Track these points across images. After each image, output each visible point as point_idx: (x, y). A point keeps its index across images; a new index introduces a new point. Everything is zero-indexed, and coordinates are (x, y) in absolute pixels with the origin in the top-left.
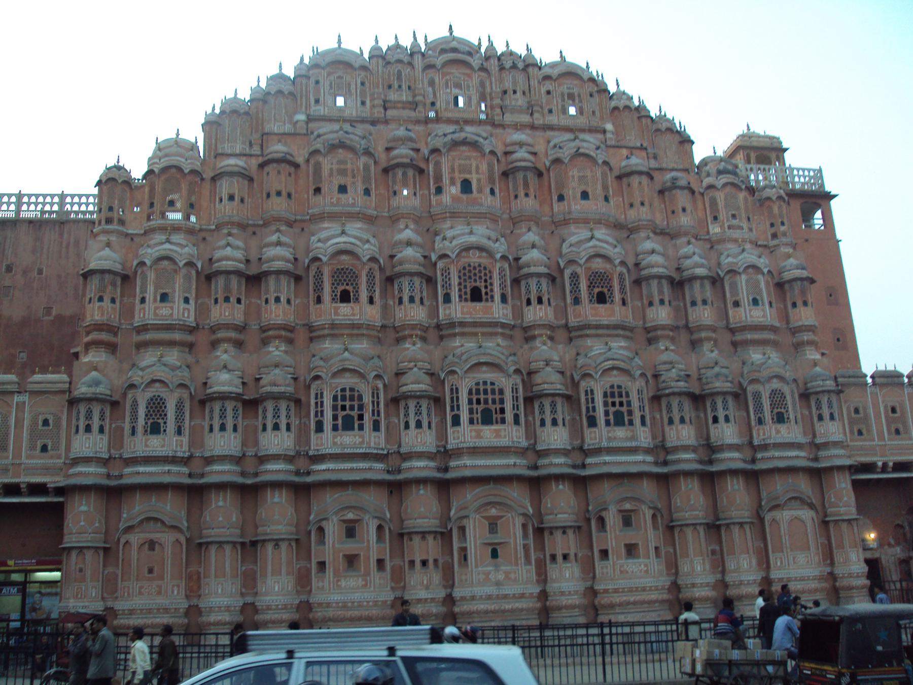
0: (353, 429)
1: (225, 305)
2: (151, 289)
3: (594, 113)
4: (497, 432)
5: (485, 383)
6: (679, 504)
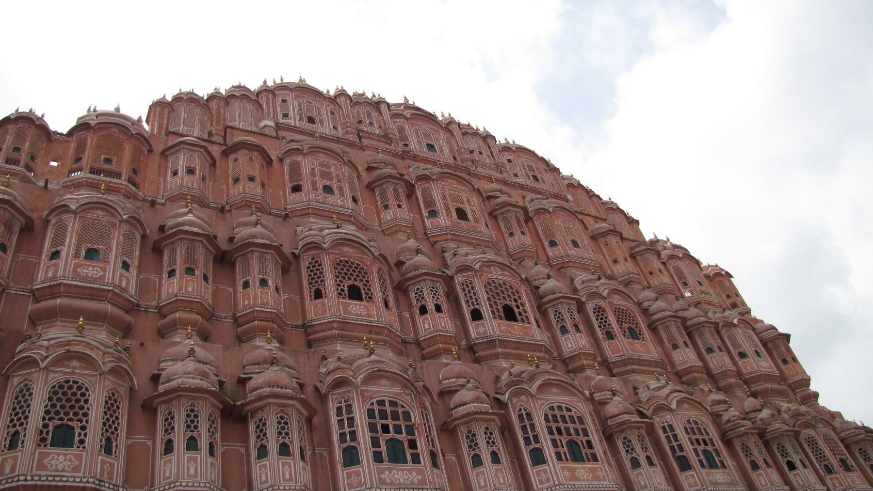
1: (187, 277)
2: (70, 241)
4: (593, 471)
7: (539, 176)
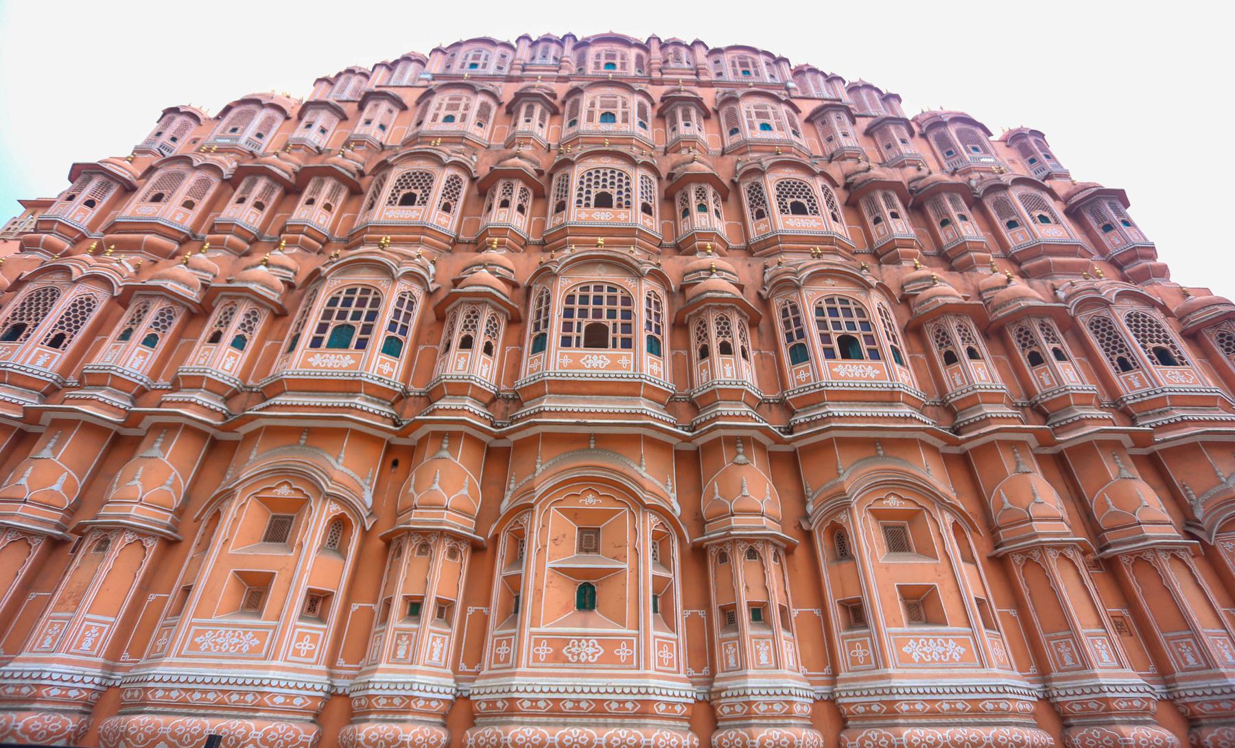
0: (346, 346)
3: (772, 76)
5: (599, 288)
6: (1007, 505)
7: (752, 69)
